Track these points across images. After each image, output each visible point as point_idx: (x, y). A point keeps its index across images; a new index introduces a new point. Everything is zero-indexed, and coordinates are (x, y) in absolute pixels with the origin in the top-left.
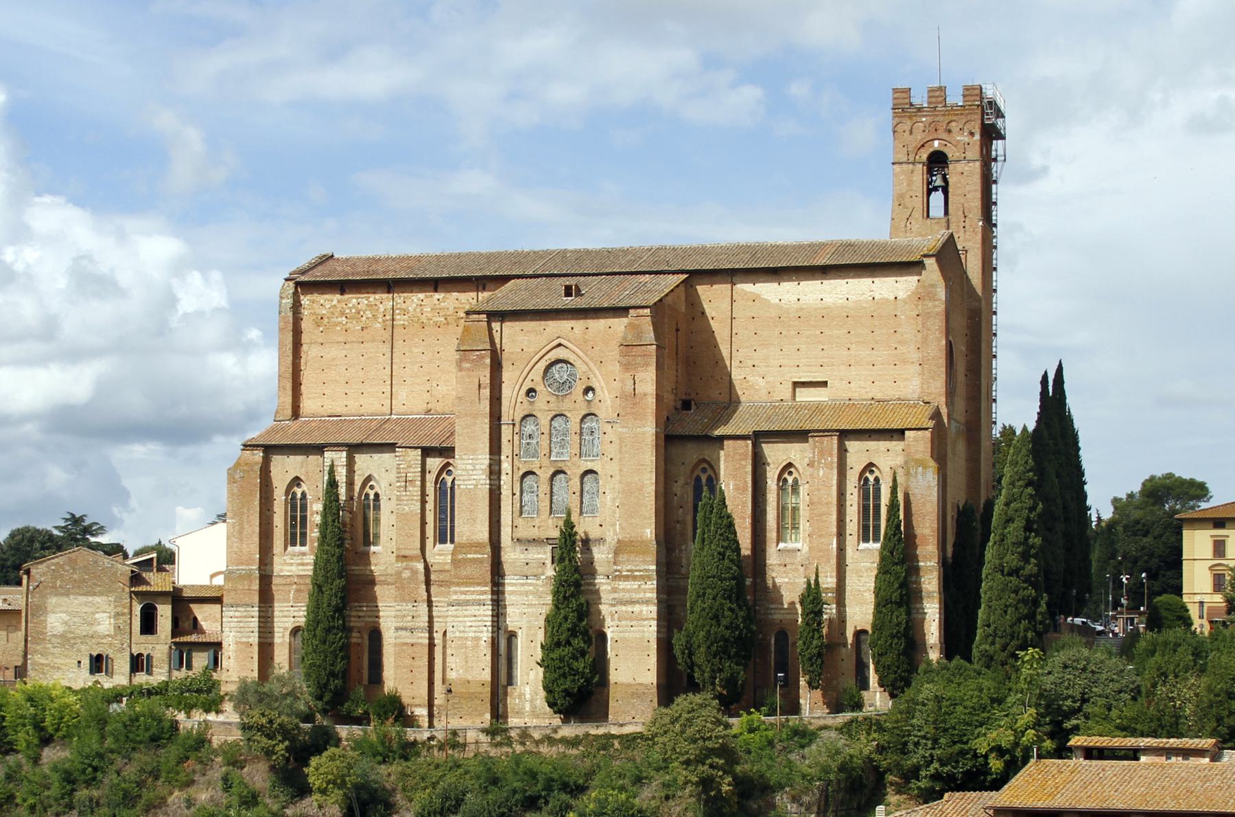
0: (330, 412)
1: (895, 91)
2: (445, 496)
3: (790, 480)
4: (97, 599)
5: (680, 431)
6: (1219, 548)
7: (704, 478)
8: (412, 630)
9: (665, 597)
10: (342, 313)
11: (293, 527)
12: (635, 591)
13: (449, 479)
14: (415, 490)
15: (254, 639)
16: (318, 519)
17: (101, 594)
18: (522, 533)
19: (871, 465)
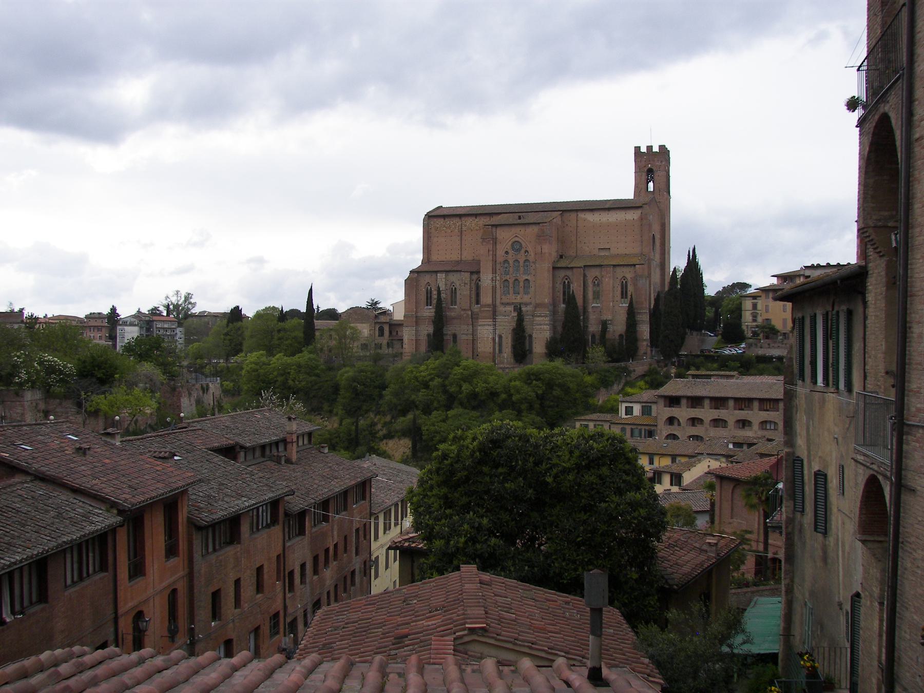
0: (441, 260)
1: (635, 147)
2: (478, 288)
3: (596, 282)
4: (364, 325)
5: (557, 266)
6: (755, 306)
7: (566, 282)
8: (467, 335)
9: (552, 323)
10: (444, 226)
11: (427, 299)
12: (543, 320)
13: (480, 283)
14: (468, 286)
15: (414, 338)
16: (436, 297)
17: (364, 323)
18: (503, 301)
19: (624, 277)
